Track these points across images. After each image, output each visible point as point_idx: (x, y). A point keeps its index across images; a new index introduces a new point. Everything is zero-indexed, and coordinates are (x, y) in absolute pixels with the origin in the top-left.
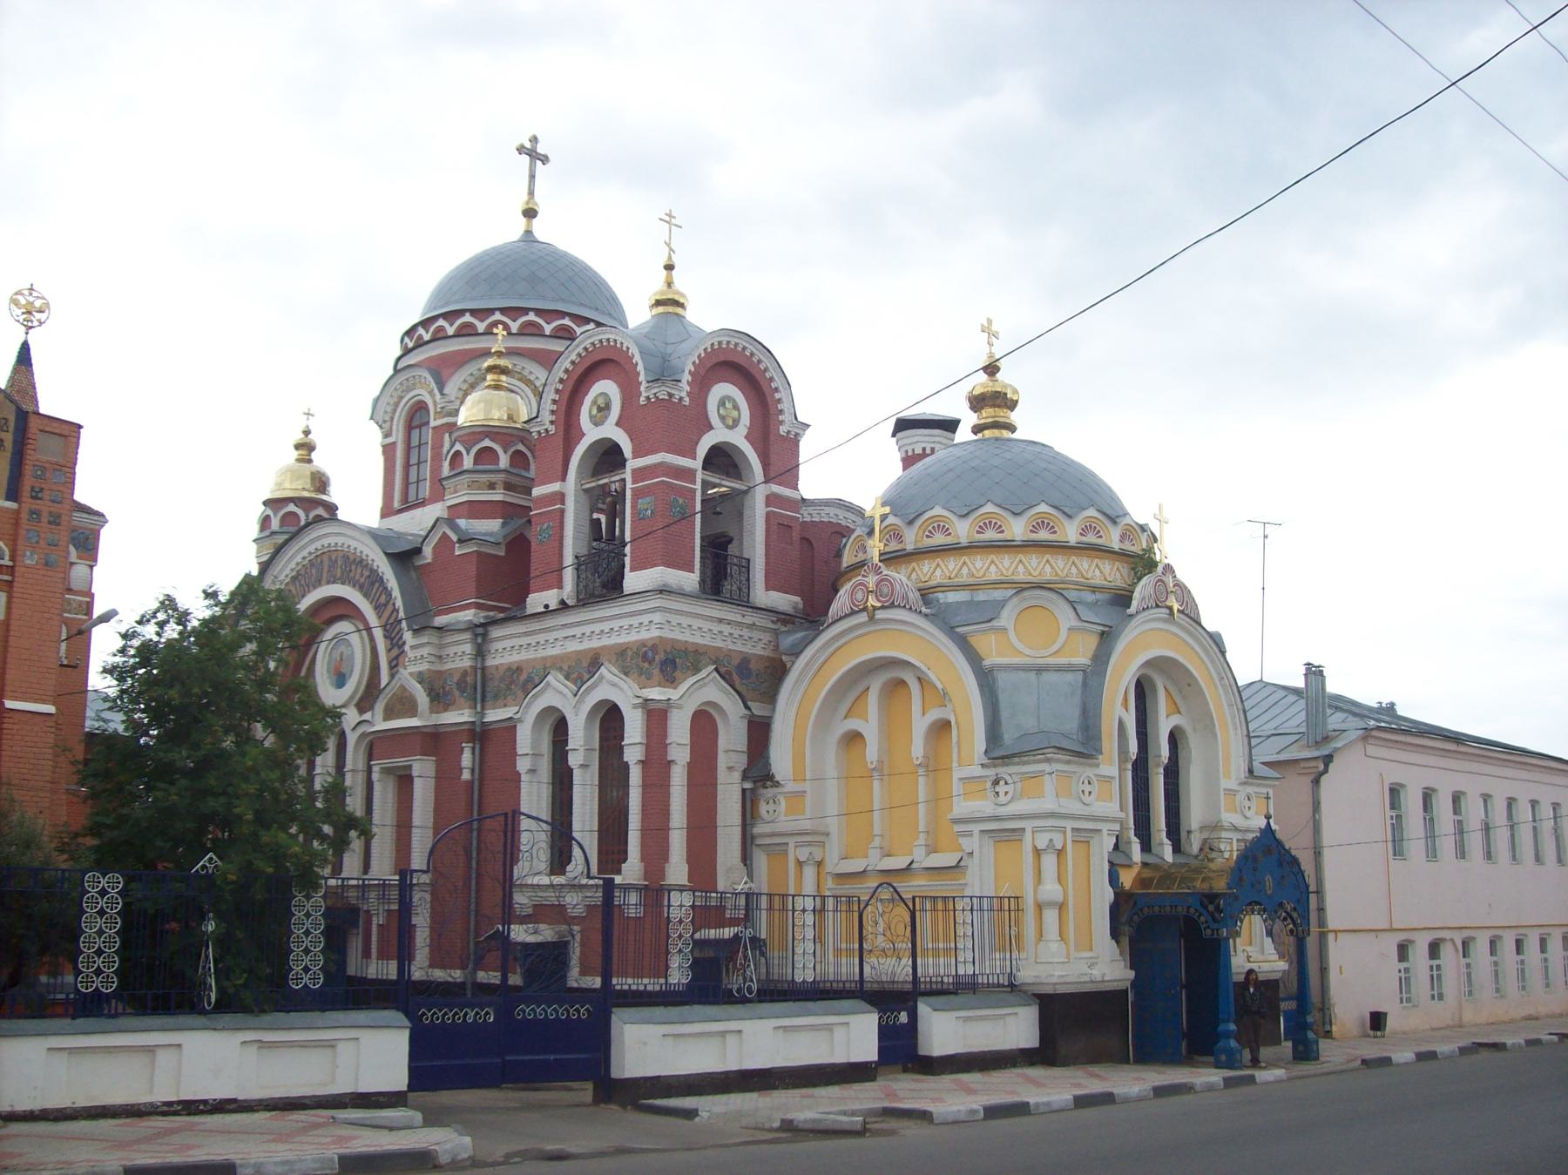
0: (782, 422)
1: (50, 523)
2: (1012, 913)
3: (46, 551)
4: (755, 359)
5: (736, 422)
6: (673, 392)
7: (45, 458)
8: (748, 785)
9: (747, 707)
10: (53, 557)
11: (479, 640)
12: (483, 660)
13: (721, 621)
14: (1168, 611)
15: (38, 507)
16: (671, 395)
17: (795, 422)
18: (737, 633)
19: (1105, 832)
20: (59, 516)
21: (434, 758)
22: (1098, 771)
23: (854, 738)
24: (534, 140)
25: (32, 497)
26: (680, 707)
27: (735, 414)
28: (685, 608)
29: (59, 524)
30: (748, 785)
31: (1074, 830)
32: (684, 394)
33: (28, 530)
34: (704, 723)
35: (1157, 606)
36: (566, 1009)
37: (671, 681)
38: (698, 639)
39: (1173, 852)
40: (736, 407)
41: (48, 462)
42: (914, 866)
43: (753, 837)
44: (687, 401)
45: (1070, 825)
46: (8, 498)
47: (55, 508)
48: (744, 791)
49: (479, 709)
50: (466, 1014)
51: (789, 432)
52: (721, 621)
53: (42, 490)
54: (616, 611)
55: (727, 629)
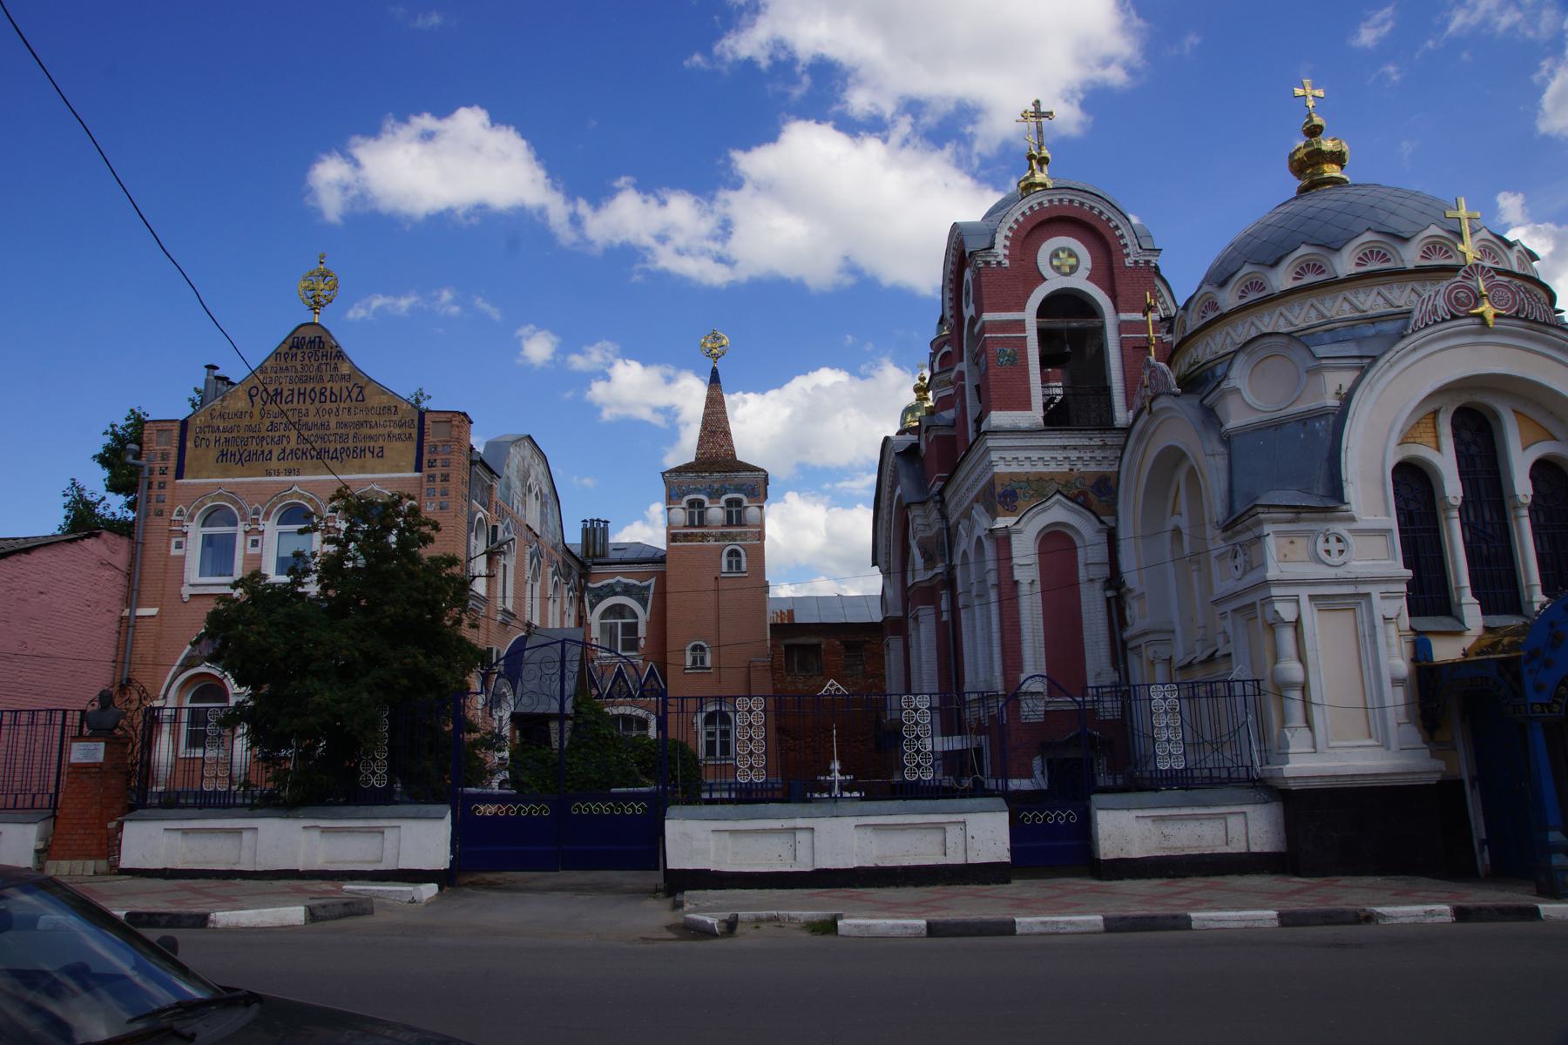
0: (1128, 255)
1: (442, 481)
2: (1250, 700)
3: (441, 500)
4: (1086, 208)
5: (1073, 269)
6: (988, 259)
7: (435, 440)
8: (1110, 594)
9: (1102, 522)
10: (445, 504)
11: (939, 506)
12: (947, 522)
13: (1065, 448)
14: (1477, 320)
15: (433, 472)
16: (988, 263)
17: (1139, 251)
18: (1086, 456)
19: (1376, 598)
20: (448, 475)
21: (933, 606)
22: (1355, 526)
23: (1177, 532)
24: (1037, 103)
25: (429, 467)
26: (1019, 532)
27: (1072, 261)
28: (1017, 443)
29: (448, 481)
30: (1110, 594)
31: (1312, 598)
32: (1001, 258)
33: (428, 489)
34: (1056, 543)
35: (1454, 317)
36: (632, 806)
37: (1011, 509)
38: (1040, 468)
39: (1483, 613)
40: (1072, 254)
41: (440, 441)
42: (1218, 654)
43: (1124, 643)
44: (1006, 263)
45: (1304, 593)
46: (416, 471)
47: (445, 470)
48: (1108, 600)
49: (947, 562)
50: (521, 808)
51: (1136, 262)
52: (1065, 448)
53: (435, 460)
54: (977, 457)
55: (1074, 455)
